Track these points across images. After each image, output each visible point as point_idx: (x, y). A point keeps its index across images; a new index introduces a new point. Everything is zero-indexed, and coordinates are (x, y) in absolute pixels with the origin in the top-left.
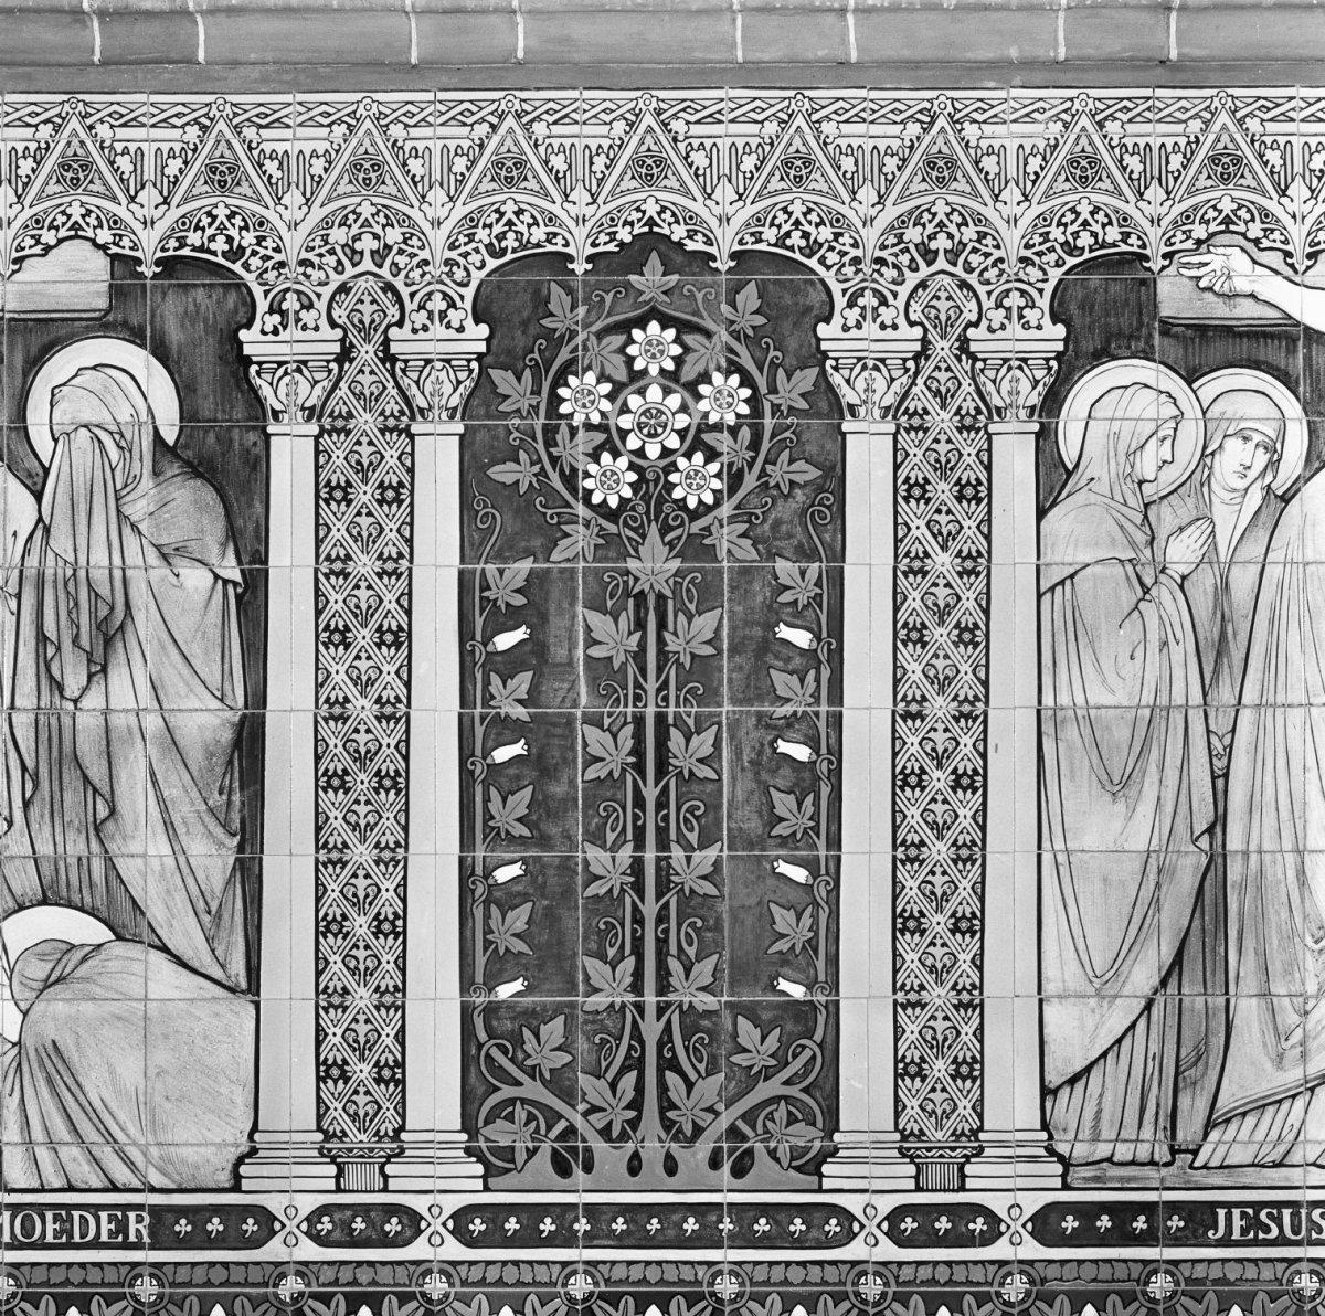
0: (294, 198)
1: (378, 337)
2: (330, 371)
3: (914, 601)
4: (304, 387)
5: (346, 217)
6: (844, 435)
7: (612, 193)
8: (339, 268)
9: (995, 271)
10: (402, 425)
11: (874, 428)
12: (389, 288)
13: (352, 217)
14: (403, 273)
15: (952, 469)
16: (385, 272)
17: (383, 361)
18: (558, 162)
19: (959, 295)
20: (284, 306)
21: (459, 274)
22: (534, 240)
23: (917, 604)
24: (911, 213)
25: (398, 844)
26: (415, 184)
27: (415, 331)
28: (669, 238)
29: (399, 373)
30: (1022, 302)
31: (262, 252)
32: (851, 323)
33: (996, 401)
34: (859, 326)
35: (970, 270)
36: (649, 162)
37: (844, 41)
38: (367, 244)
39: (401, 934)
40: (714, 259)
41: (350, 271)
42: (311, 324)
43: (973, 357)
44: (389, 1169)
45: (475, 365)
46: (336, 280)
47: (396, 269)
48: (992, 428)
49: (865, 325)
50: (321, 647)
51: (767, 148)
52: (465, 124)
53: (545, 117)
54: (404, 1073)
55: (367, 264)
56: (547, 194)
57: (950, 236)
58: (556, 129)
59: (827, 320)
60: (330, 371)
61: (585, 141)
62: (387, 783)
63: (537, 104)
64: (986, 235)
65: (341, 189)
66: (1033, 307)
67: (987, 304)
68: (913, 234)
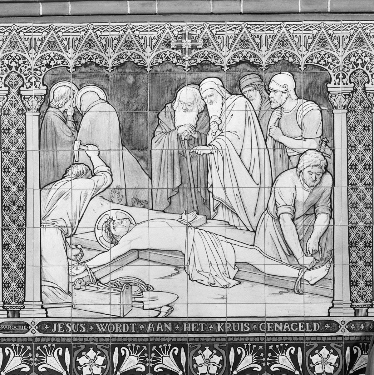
0: (71, 51)
1: (17, 88)
2: (4, 98)
3: (353, 158)
4: (36, 103)
5: (8, 57)
6: (333, 114)
7: (118, 50)
8: (6, 71)
9: (28, 71)
10: (22, 112)
11: (34, 114)
12: (19, 76)
13: (10, 57)
14: (22, 72)
15: (16, 125)
16: (18, 72)
17: (18, 95)
18: (103, 42)
19: (356, 74)
20: (31, 81)
21: (346, 69)
22: (58, 63)
23: (7, 161)
24: (6, 56)
25: (23, 224)
26: (103, 47)
27: (335, 84)
28: (95, 63)
29: (23, 99)
30: (343, 77)
31: (25, 66)
32: (337, 83)
33: (335, 105)
34: (339, 84)
35: (21, 71)
36: (128, 42)
37: (213, 6)
38: (14, 64)
39: (24, 248)
40: (185, 67)
41: (9, 71)
42: (38, 86)
43: (21, 95)
44: (21, 312)
45: (43, 97)
46: (6, 75)
47: (21, 71)
48: (26, 114)
49: (340, 84)
50: (3, 173)
51: (5, 39)
52: (40, 32)
53: (61, 30)
54: (350, 283)
55: (14, 69)
56: (255, 49)
57: (16, 63)
58: (65, 34)
59: (330, 83)
60: (42, 98)
61: (342, 35)
62: (21, 208)
63: (253, 26)
64: (25, 62)
65: (84, 48)
66: (38, 81)
67: (26, 81)
68: (45, 62)
